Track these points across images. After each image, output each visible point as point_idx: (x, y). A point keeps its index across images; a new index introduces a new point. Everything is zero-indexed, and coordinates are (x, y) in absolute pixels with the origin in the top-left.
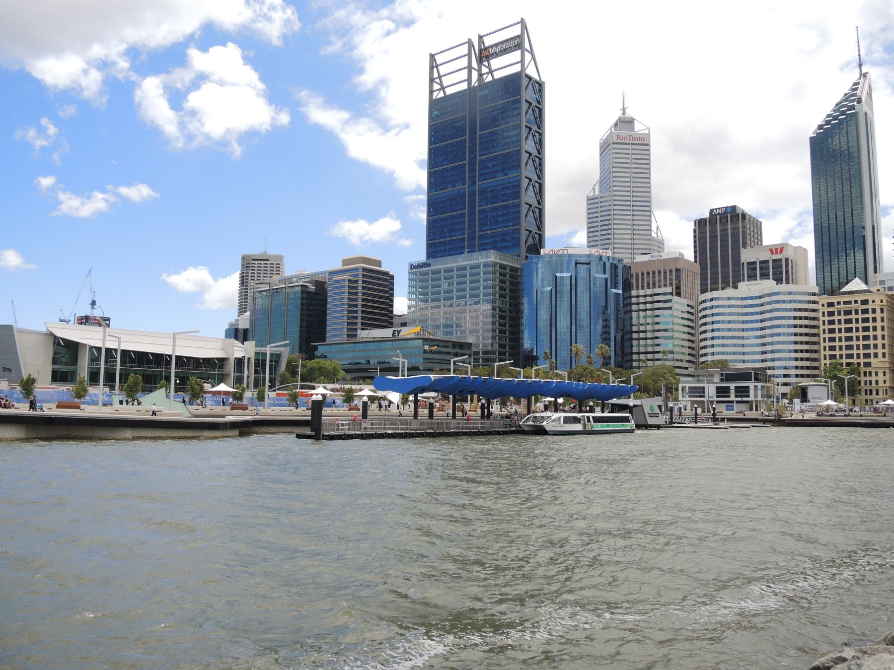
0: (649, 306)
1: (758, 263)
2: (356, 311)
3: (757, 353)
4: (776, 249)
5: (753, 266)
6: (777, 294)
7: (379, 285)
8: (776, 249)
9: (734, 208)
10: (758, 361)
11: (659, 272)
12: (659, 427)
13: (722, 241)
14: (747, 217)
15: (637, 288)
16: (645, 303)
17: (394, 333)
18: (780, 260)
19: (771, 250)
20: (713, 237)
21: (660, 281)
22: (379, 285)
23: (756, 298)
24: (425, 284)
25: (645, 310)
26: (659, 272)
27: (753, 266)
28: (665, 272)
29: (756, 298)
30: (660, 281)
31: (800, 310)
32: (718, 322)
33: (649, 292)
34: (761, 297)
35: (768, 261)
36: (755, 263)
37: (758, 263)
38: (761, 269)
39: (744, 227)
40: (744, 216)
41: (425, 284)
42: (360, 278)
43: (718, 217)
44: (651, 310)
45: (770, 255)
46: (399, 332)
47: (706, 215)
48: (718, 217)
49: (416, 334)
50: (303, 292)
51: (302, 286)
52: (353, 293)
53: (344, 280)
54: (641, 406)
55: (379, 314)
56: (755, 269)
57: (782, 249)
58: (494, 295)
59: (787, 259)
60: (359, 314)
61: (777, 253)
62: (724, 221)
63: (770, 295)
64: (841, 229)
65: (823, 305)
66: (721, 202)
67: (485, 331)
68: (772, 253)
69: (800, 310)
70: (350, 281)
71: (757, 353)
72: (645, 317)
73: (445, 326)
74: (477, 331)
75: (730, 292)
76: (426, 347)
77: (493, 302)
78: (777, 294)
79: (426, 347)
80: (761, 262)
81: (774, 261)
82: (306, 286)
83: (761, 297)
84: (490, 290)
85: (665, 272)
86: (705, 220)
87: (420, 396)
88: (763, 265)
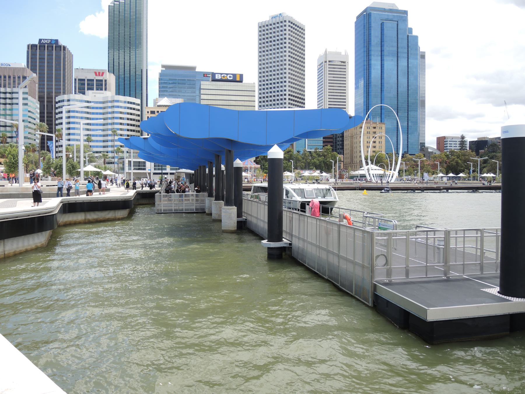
0: (8, 101)
1: (86, 80)
3: (100, 141)
4: (99, 73)
5: (82, 82)
6: (118, 101)
8: (99, 73)
9: (57, 41)
10: (101, 147)
11: (9, 77)
13: (48, 63)
14: (66, 50)
15: (5, 86)
16: (5, 98)
18: (102, 81)
19: (96, 73)
20: (42, 59)
21: (9, 84)
23: (100, 103)
25: (5, 104)
26: (9, 77)
27: (82, 82)
28: (14, 78)
29: (100, 103)
30: (9, 84)
31: (131, 114)
32: (74, 117)
33: (9, 90)
34: (103, 103)
35: (93, 80)
36: (84, 80)
37: (86, 80)
38: (88, 85)
39: (64, 55)
40: (64, 48)
43: (46, 45)
44: (10, 104)
45: (95, 76)
47: (37, 43)
48: (46, 45)
56: (84, 84)
57: (103, 73)
59: (106, 81)
61: (99, 75)
62: (50, 48)
63: (111, 102)
64: (127, 68)
65: (148, 112)
66: (48, 35)
68: (96, 75)
69: (131, 114)
71: (100, 141)
72: (5, 110)
75: (79, 96)
78: (118, 101)
80: (88, 80)
81: (97, 80)
83: (103, 103)
85: (14, 78)
86: (36, 46)
88: (90, 82)
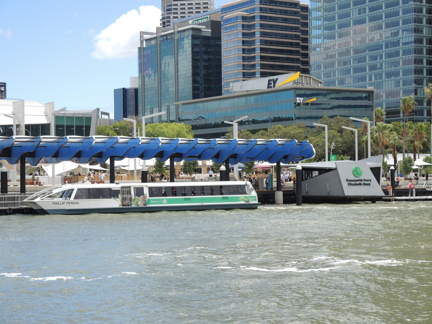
2: (254, 58)
7: (285, 20)
12: (373, 199)
17: (269, 84)
22: (285, 20)
24: (331, 14)
41: (331, 14)
42: (257, 13)
46: (275, 82)
49: (295, 82)
50: (194, 37)
51: (193, 29)
52: (248, 35)
53: (237, 18)
54: (336, 169)
55: (287, 60)
58: (418, 21)
60: (258, 61)
67: (405, 72)
70: (244, 18)
73: (356, 70)
74: (396, 74)
76: (299, 100)
77: (417, 30)
79: (299, 100)
82: (199, 30)
84: (412, 15)
87: (117, 163)
